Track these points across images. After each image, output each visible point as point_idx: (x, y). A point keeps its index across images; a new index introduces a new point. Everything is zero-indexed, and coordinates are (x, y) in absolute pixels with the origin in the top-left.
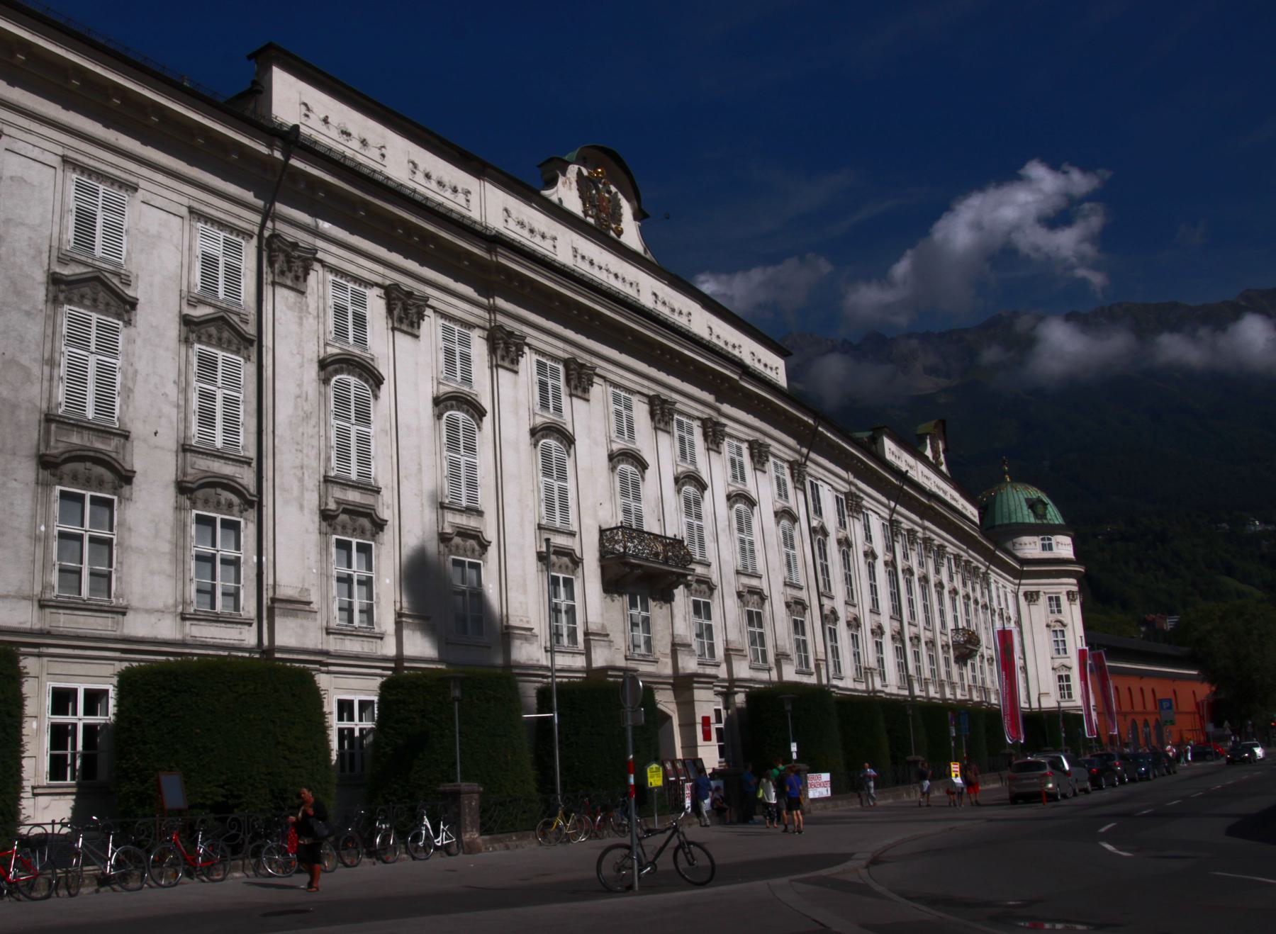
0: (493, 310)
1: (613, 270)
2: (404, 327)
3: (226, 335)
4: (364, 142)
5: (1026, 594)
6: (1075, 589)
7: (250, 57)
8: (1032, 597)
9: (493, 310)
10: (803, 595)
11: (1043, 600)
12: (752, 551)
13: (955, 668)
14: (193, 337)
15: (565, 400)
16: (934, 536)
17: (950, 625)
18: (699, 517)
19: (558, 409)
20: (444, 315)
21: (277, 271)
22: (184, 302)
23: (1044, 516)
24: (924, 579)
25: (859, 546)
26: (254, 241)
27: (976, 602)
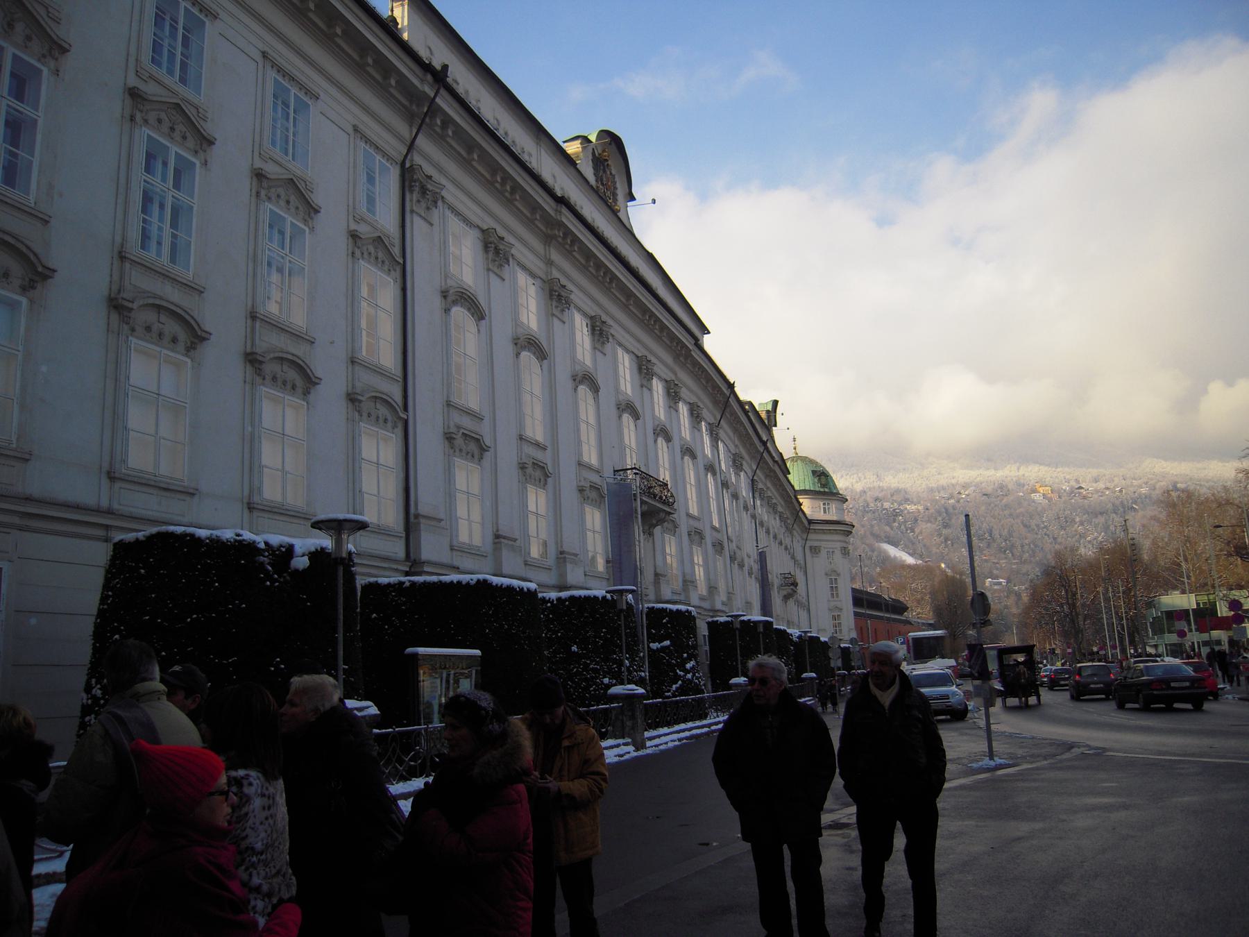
0: (550, 263)
2: (495, 269)
3: (380, 255)
9: (550, 263)
22: (351, 218)
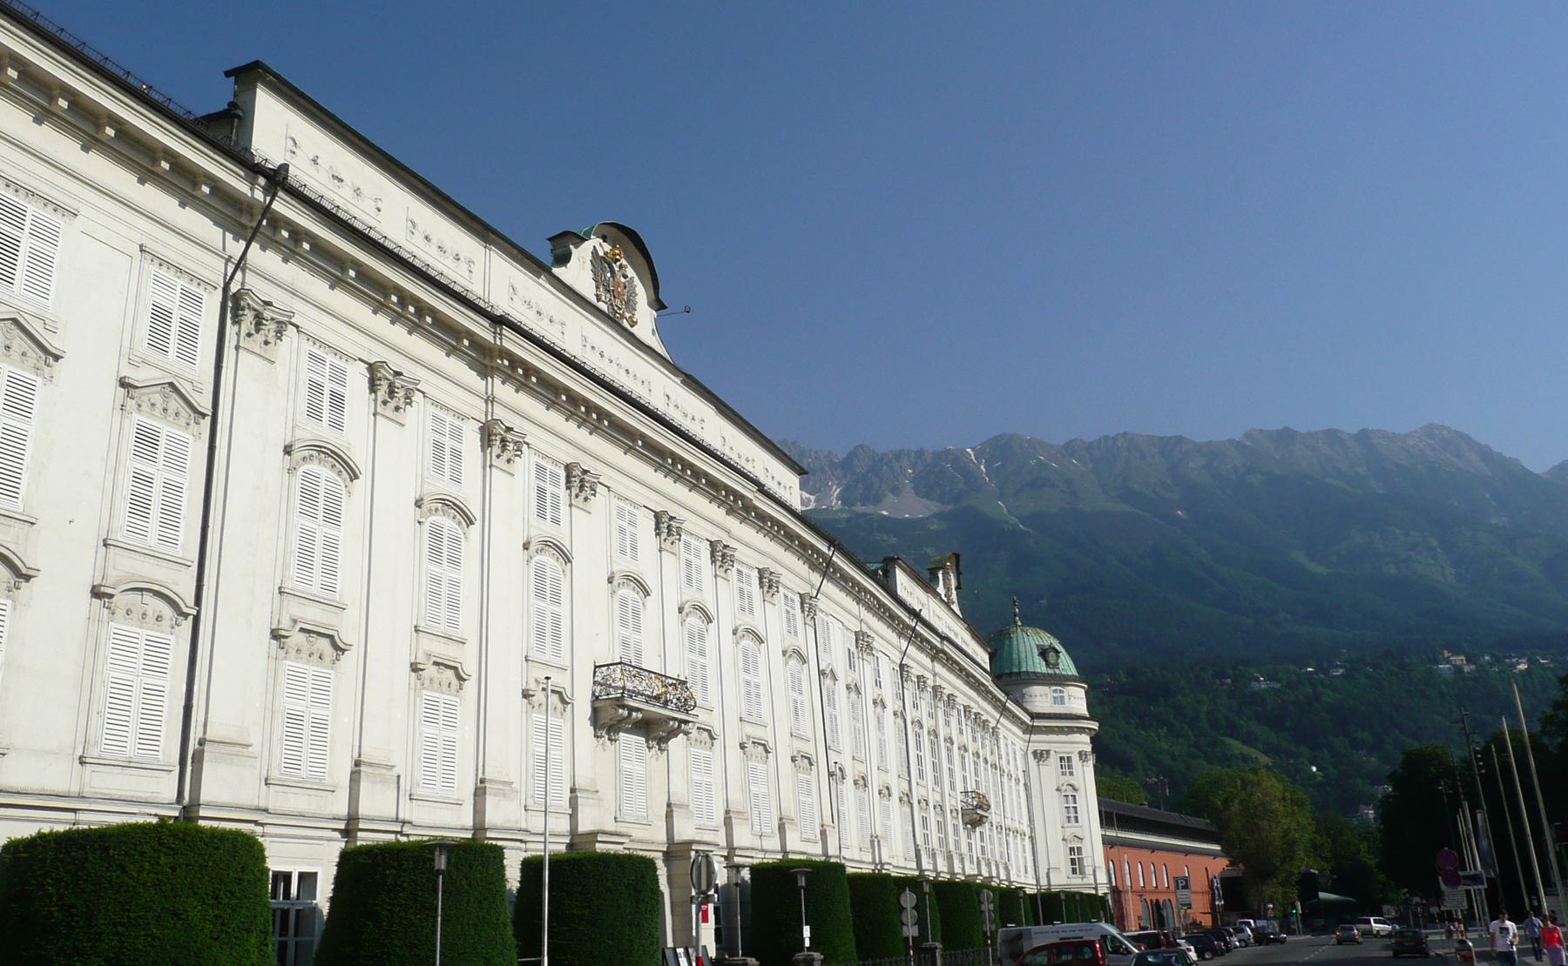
1: (625, 365)
4: (357, 191)
5: (1035, 753)
6: (1088, 748)
7: (228, 74)
8: (1040, 756)
9: (490, 400)
10: (808, 748)
11: (1054, 760)
12: (758, 695)
13: (963, 834)
14: (131, 404)
15: (564, 508)
16: (944, 684)
17: (960, 787)
18: (702, 653)
19: (556, 521)
20: (435, 403)
21: (243, 334)
22: (124, 361)
23: (1056, 665)
24: (934, 733)
25: (870, 692)
26: (219, 294)
27: (986, 761)
